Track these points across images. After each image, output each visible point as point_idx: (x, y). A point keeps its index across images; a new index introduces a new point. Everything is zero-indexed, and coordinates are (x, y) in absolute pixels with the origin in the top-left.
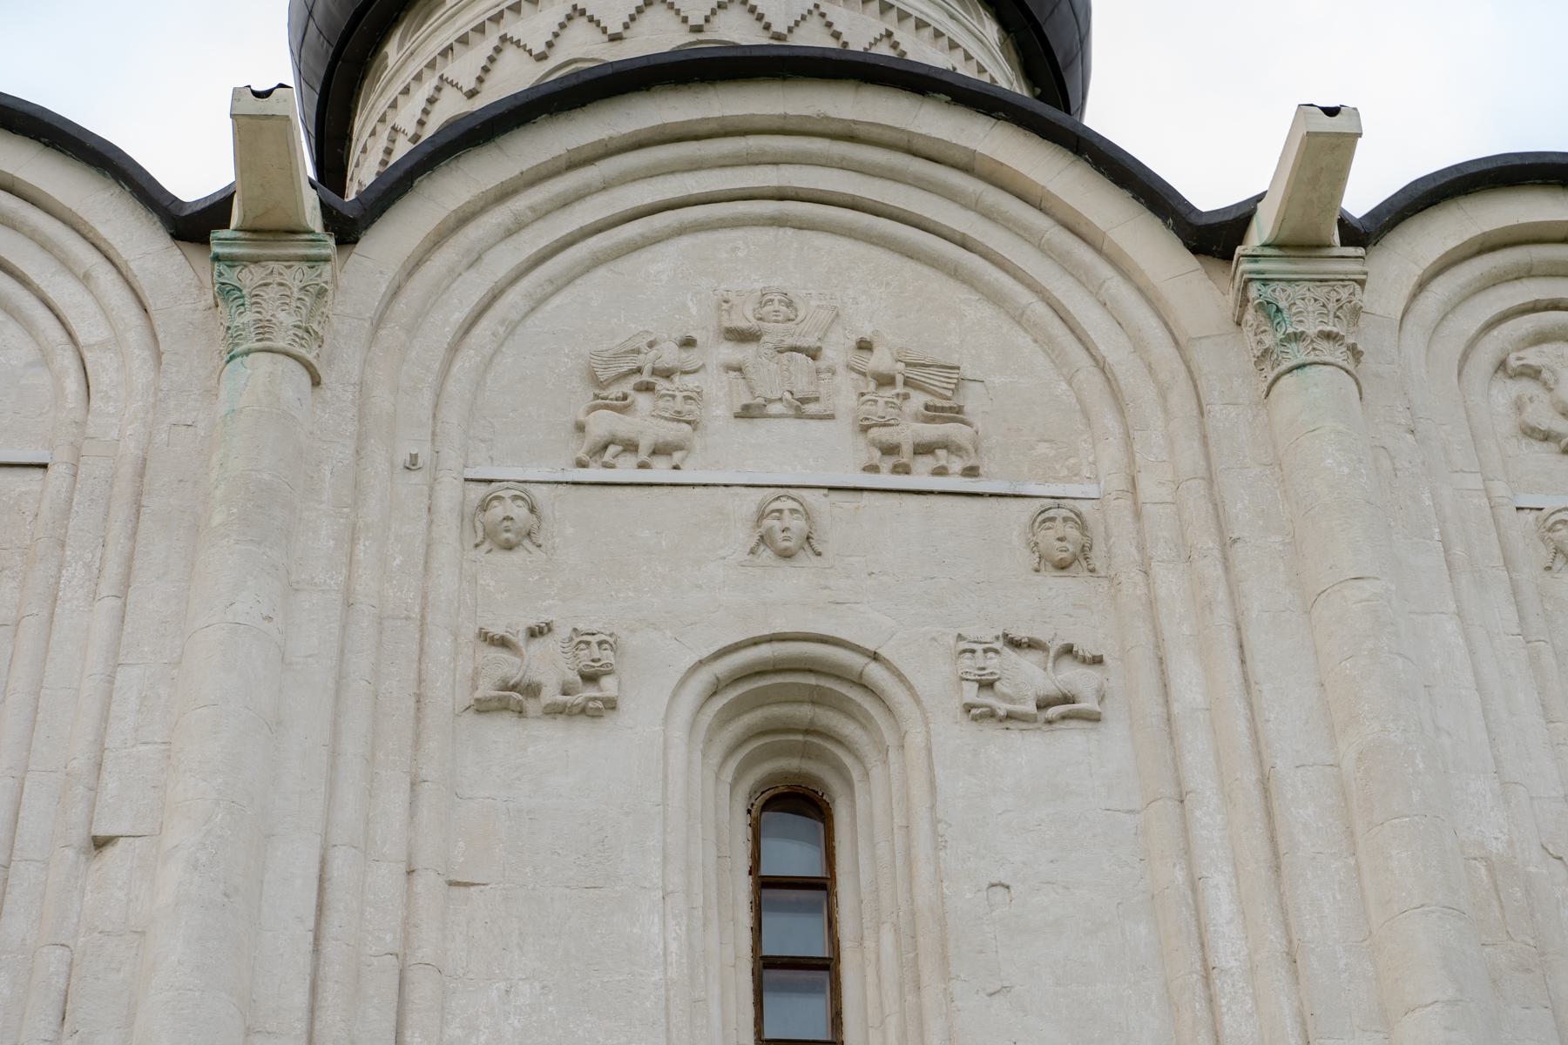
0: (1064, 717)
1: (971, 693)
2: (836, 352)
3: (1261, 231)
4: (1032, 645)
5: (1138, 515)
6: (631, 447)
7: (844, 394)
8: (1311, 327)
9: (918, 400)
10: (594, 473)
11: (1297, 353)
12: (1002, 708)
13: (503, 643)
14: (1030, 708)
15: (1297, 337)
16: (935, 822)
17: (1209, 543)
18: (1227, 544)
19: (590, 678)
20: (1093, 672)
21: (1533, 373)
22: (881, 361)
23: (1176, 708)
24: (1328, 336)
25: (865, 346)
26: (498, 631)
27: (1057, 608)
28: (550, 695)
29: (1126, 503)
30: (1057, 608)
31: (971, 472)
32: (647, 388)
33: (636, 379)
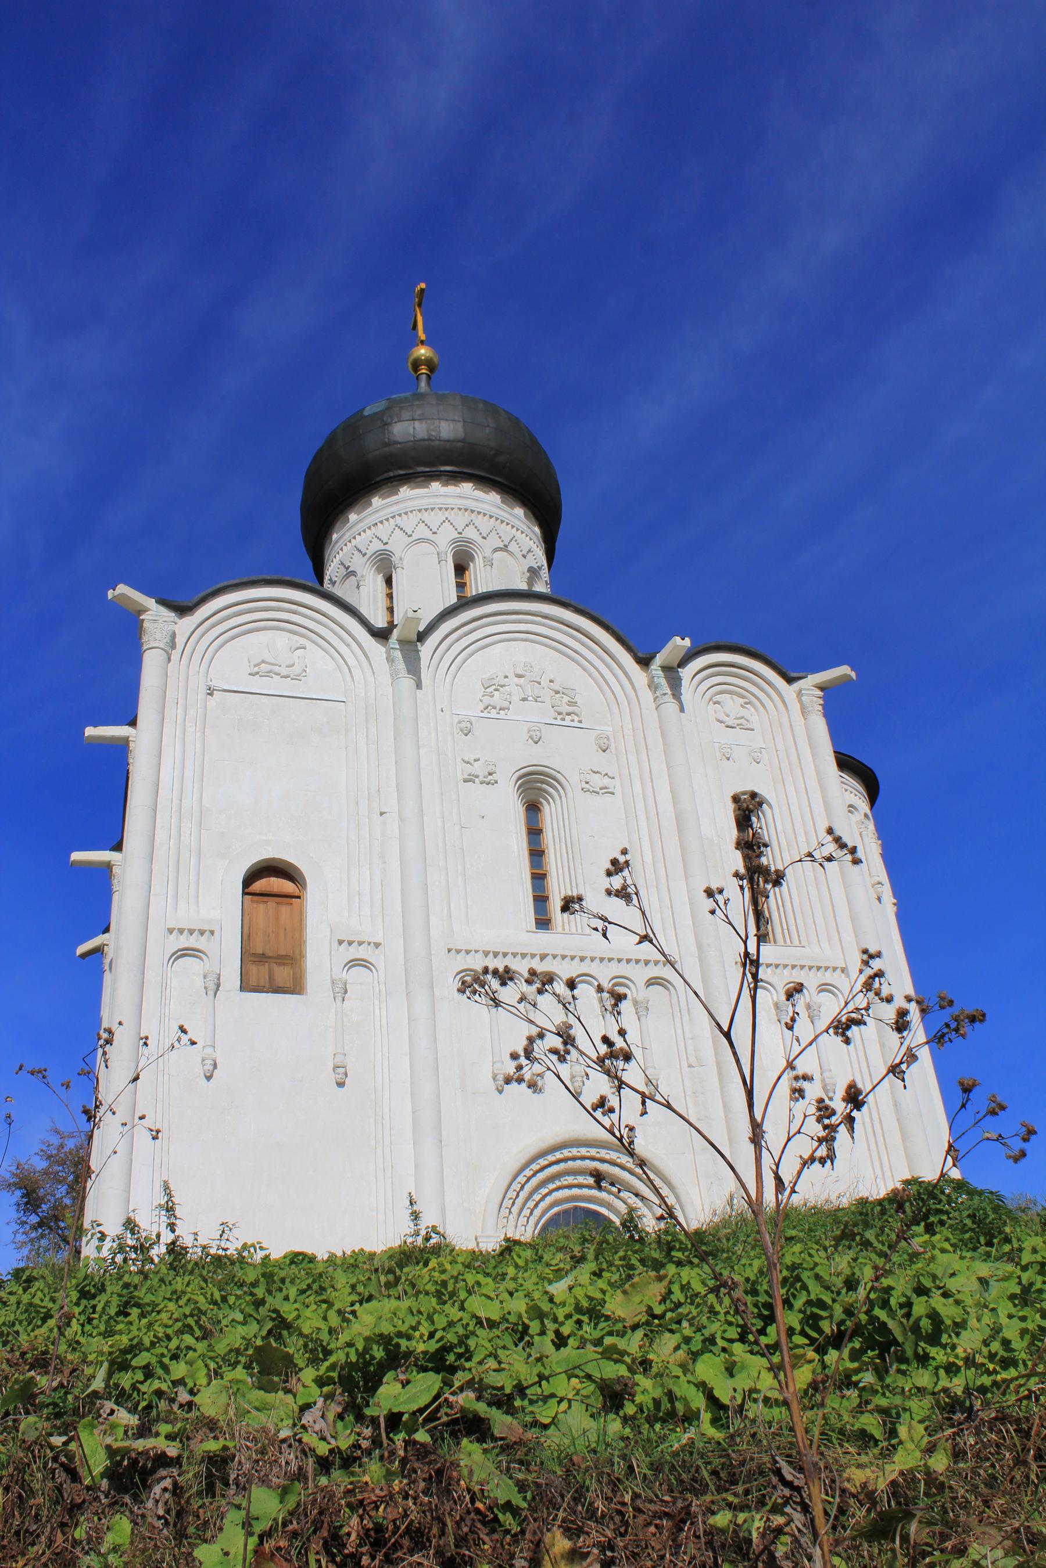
2: (545, 682)
4: (598, 772)
6: (494, 708)
7: (547, 695)
9: (566, 699)
10: (483, 715)
12: (591, 789)
13: (468, 763)
19: (490, 774)
22: (555, 686)
25: (551, 681)
26: (467, 759)
27: (601, 762)
28: (481, 778)
30: (601, 762)
31: (580, 722)
32: (496, 690)
33: (494, 687)
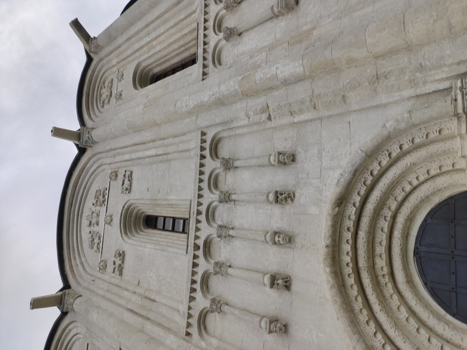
0: (131, 177)
1: (127, 192)
3: (77, 143)
5: (112, 163)
8: (88, 135)
11: (90, 138)
14: (129, 182)
15: (89, 138)
16: (140, 200)
17: (112, 152)
18: (112, 150)
20: (127, 172)
21: (103, 102)
23: (129, 159)
24: (89, 133)
29: (111, 165)
